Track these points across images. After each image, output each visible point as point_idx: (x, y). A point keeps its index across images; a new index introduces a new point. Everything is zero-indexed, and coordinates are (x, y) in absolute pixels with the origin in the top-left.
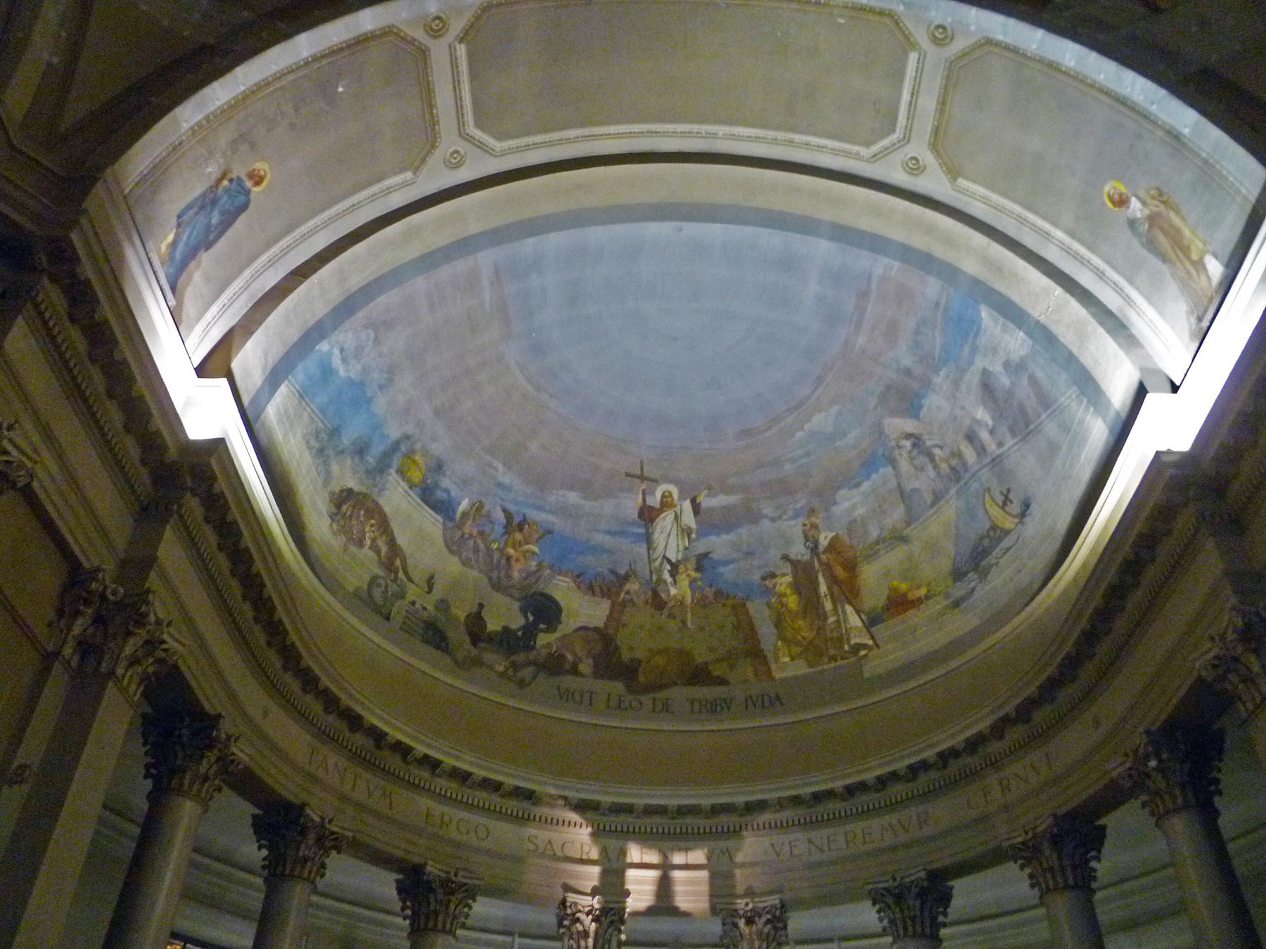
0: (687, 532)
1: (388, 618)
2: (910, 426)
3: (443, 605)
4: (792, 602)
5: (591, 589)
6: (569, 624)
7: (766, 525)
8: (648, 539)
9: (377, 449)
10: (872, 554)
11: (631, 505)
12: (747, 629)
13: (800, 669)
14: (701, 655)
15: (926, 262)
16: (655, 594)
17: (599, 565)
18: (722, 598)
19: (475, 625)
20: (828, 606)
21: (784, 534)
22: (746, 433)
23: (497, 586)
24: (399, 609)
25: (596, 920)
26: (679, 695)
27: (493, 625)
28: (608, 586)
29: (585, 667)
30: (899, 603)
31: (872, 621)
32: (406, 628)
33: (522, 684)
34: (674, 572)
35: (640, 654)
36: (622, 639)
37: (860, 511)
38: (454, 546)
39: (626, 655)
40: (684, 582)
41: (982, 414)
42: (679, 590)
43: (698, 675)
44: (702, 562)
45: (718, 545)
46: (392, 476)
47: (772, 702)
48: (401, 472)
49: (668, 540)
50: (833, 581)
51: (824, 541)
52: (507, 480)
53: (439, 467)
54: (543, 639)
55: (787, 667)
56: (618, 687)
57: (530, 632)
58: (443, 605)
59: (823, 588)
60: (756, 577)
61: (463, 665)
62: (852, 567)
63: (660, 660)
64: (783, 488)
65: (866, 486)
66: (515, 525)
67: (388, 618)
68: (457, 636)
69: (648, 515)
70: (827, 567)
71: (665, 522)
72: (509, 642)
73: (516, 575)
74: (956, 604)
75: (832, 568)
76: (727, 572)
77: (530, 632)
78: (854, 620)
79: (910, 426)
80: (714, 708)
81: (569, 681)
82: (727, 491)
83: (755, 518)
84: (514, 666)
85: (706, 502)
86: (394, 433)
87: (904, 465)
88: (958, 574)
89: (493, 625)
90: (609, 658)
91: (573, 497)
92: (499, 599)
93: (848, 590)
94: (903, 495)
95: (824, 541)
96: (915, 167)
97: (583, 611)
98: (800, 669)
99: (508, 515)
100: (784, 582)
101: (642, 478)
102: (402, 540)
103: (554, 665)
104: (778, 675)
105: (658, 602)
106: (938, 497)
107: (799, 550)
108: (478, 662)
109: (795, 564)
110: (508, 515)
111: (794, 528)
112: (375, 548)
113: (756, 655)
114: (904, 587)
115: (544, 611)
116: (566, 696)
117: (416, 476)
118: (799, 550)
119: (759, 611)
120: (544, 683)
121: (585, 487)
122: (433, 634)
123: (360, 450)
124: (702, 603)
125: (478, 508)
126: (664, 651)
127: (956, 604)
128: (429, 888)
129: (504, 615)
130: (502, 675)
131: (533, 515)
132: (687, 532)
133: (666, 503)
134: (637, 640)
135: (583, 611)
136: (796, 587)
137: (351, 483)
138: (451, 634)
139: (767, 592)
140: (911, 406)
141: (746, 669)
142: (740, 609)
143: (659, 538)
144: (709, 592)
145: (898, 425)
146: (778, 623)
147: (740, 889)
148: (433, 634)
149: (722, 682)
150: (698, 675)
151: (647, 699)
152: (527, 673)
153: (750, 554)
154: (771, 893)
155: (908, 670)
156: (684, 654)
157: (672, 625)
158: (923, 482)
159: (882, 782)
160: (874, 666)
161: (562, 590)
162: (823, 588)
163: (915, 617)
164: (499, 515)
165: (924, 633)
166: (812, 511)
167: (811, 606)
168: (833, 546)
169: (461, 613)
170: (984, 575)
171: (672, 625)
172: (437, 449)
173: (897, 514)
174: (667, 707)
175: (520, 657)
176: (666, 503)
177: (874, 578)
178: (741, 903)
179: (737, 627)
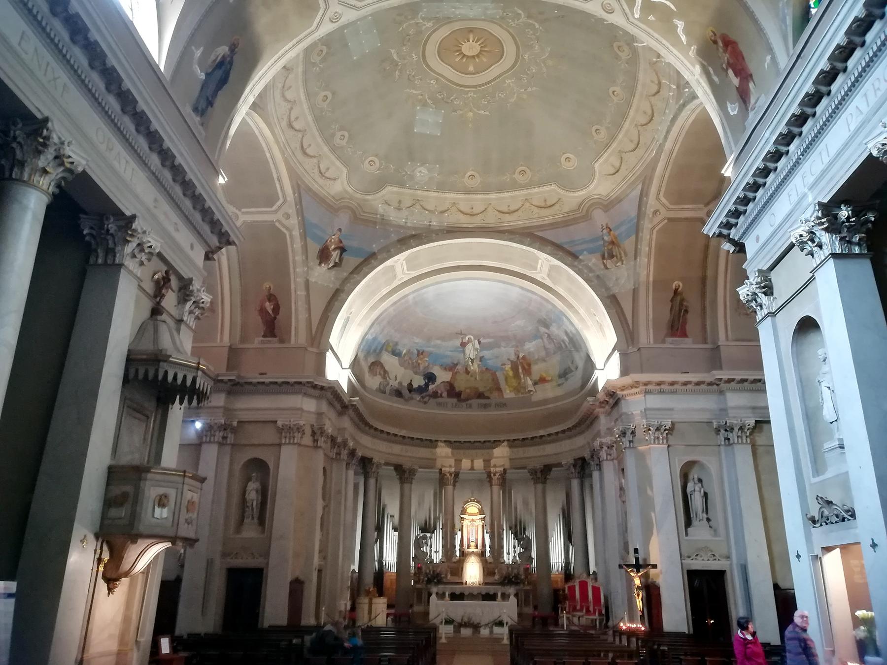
0: (476, 349)
1: (385, 393)
2: (547, 331)
3: (400, 383)
4: (511, 373)
5: (445, 369)
6: (439, 381)
7: (503, 348)
8: (464, 352)
9: (379, 348)
10: (536, 363)
11: (458, 342)
12: (495, 380)
13: (512, 395)
14: (481, 389)
15: (547, 301)
16: (466, 369)
17: (448, 361)
18: (488, 371)
19: (410, 388)
20: (522, 376)
21: (508, 352)
22: (495, 322)
23: (416, 373)
24: (388, 389)
25: (451, 475)
26: (475, 402)
27: (415, 385)
28: (452, 367)
29: (445, 394)
30: (542, 380)
31: (535, 384)
32: (390, 394)
33: (425, 403)
34: (472, 362)
35: (462, 389)
36: (456, 385)
37: (532, 349)
38: (401, 365)
39: (457, 390)
40: (476, 366)
41: (565, 338)
42: (474, 368)
43: (480, 395)
44: (481, 359)
45: (487, 354)
46: (384, 352)
47: (502, 405)
48: (386, 350)
49: (471, 351)
50: (523, 368)
51: (521, 355)
52: (417, 340)
53: (397, 344)
54: (431, 387)
55: (508, 394)
56: (454, 400)
57: (427, 385)
58: (400, 383)
59: (520, 370)
60: (499, 365)
61: (406, 400)
62: (529, 365)
63: (468, 391)
64: (507, 339)
65: (534, 343)
66: (420, 353)
67: (385, 393)
68: (405, 392)
69: (463, 345)
70: (521, 363)
71: (469, 347)
72: (421, 390)
73: (421, 368)
74: (559, 385)
75: (522, 366)
76: (490, 363)
77: (427, 385)
78: (530, 382)
79: (547, 331)
80: (485, 406)
81: (440, 400)
82: (489, 337)
83: (499, 347)
84: (423, 398)
85: (482, 341)
86: (384, 341)
87: (545, 340)
88: (560, 377)
89: (415, 385)
90: (452, 391)
91: (439, 342)
92: (418, 377)
93: (528, 372)
94: (545, 348)
95: (521, 355)
96: (543, 278)
97: (443, 376)
98: (512, 395)
99: (418, 351)
100: (508, 367)
101: (461, 334)
102: (387, 368)
103: (435, 395)
104: (506, 396)
105: (467, 372)
106: (554, 353)
107: (513, 358)
108: (412, 398)
109: (512, 362)
110: (418, 351)
111: (512, 351)
112: (380, 374)
113: (499, 389)
114: (544, 375)
115: (430, 378)
116: (439, 404)
117: (390, 349)
118: (513, 358)
119: (499, 375)
120: (432, 401)
121: (443, 339)
122: (398, 393)
123: (375, 351)
124: (482, 372)
125: (409, 352)
126: (470, 388)
127: (559, 385)
128: (404, 471)
129: (419, 381)
130: (419, 401)
131: (426, 349)
132: (476, 349)
133: (469, 341)
134: (461, 384)
135: (443, 376)
136: (512, 368)
137: (373, 360)
138: (403, 392)
139: (502, 369)
140: (547, 326)
141: (495, 394)
142: (494, 374)
143: (467, 352)
144: (484, 369)
145: (543, 330)
146: (506, 379)
147: (492, 465)
148: (398, 393)
149: (488, 398)
150: (480, 395)
151: (464, 404)
152: (426, 399)
153: (497, 357)
154: (500, 466)
155: (545, 402)
156: (477, 388)
157: (473, 379)
158: (551, 346)
159: (533, 438)
160: (535, 398)
161: (436, 370)
162: (520, 370)
163: (547, 386)
164: (416, 352)
165: (548, 392)
166: (517, 347)
167: (516, 375)
168: (524, 357)
169: (405, 384)
170: (566, 380)
171: (473, 379)
172: (396, 340)
173: (543, 353)
174: (470, 406)
175: (424, 395)
176: (469, 341)
177: (537, 369)
178: (492, 469)
179: (493, 380)
